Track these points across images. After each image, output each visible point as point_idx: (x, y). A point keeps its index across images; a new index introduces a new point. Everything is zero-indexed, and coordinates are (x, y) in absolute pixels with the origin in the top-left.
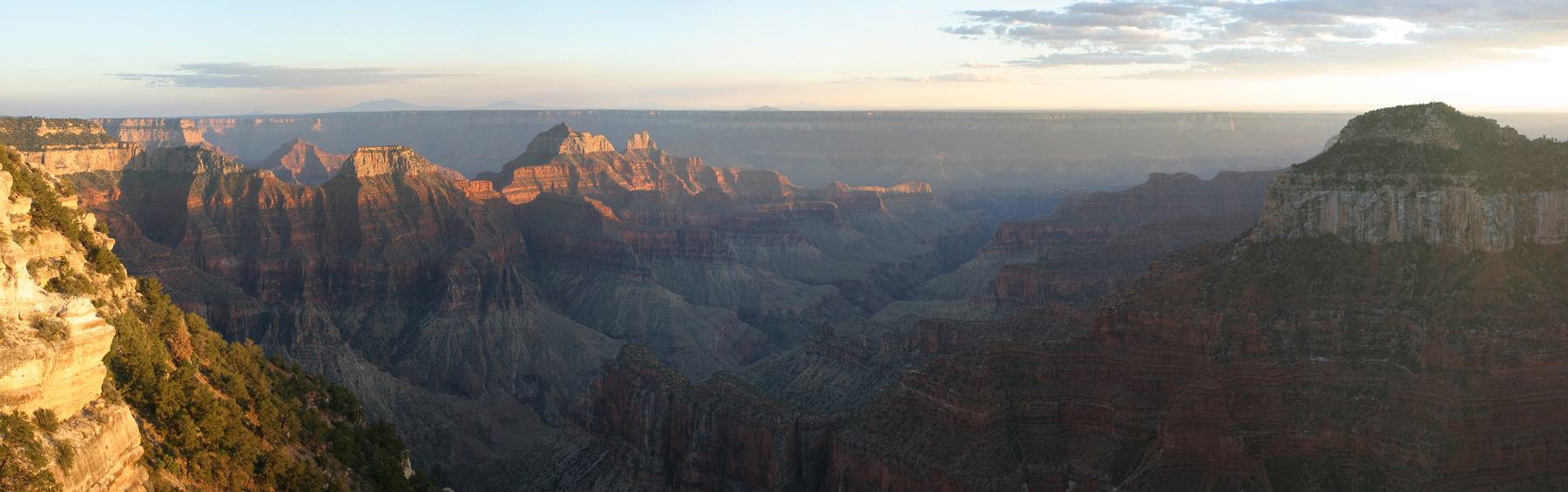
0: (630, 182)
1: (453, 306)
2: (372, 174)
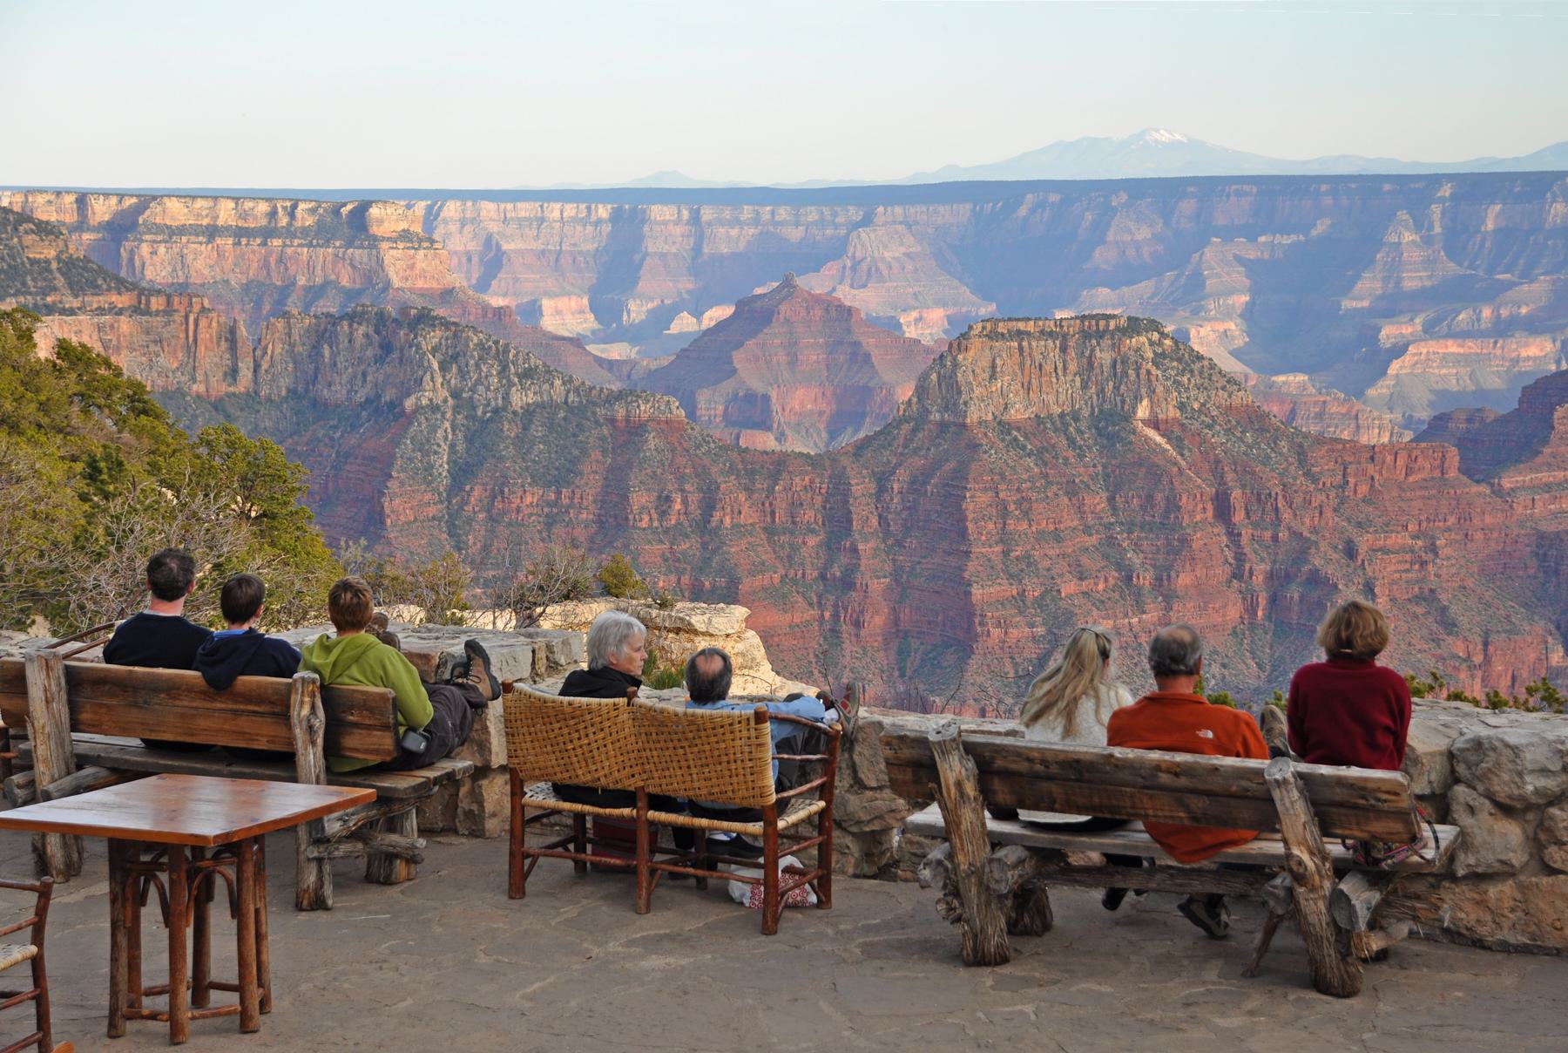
2: (1019, 412)
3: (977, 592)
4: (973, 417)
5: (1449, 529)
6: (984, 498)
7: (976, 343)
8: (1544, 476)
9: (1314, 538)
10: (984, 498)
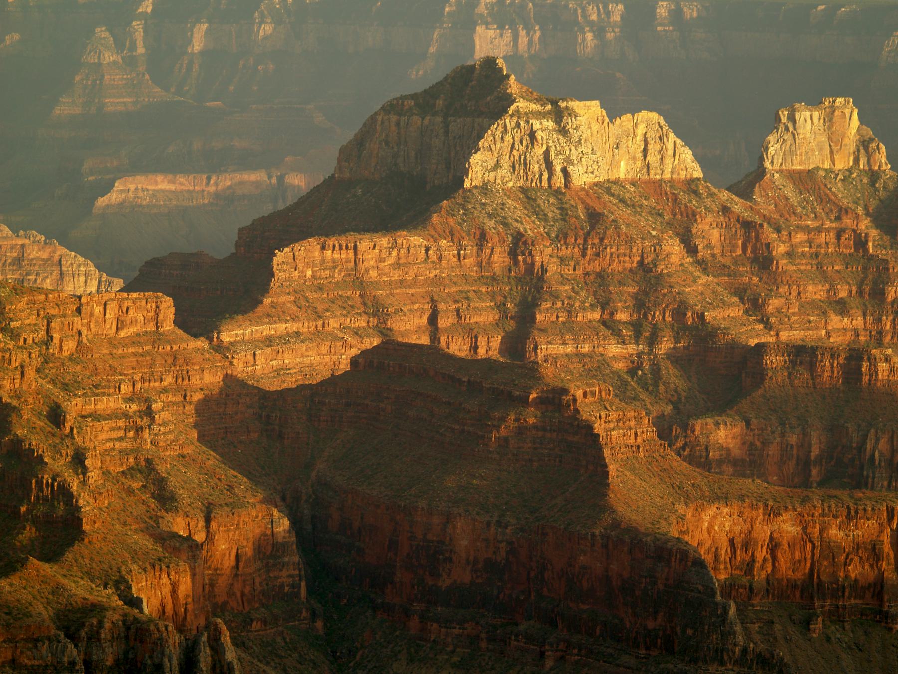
0: (755, 306)
5: (165, 390)
8: (266, 330)
9: (15, 403)
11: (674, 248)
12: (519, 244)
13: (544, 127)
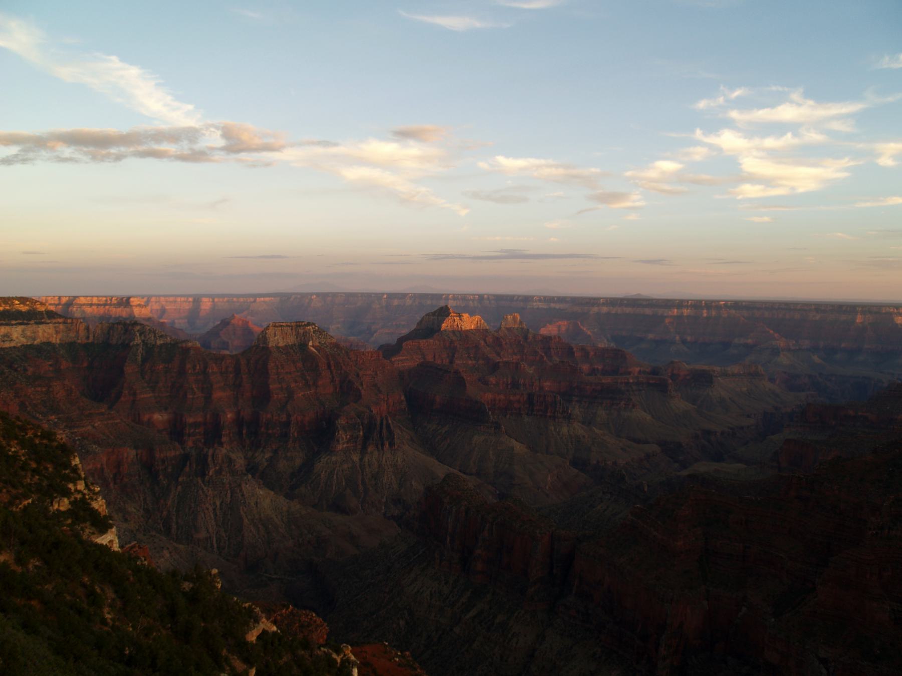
0: (498, 354)
1: (340, 447)
2: (281, 344)
3: (271, 386)
4: (270, 345)
6: (273, 365)
7: (271, 328)
10: (273, 365)
11: (482, 342)
12: (452, 342)
13: (457, 319)
